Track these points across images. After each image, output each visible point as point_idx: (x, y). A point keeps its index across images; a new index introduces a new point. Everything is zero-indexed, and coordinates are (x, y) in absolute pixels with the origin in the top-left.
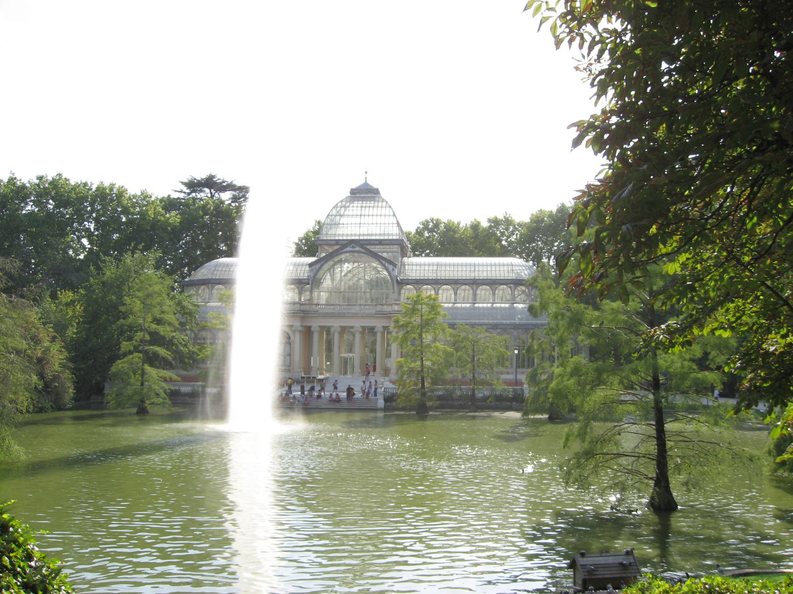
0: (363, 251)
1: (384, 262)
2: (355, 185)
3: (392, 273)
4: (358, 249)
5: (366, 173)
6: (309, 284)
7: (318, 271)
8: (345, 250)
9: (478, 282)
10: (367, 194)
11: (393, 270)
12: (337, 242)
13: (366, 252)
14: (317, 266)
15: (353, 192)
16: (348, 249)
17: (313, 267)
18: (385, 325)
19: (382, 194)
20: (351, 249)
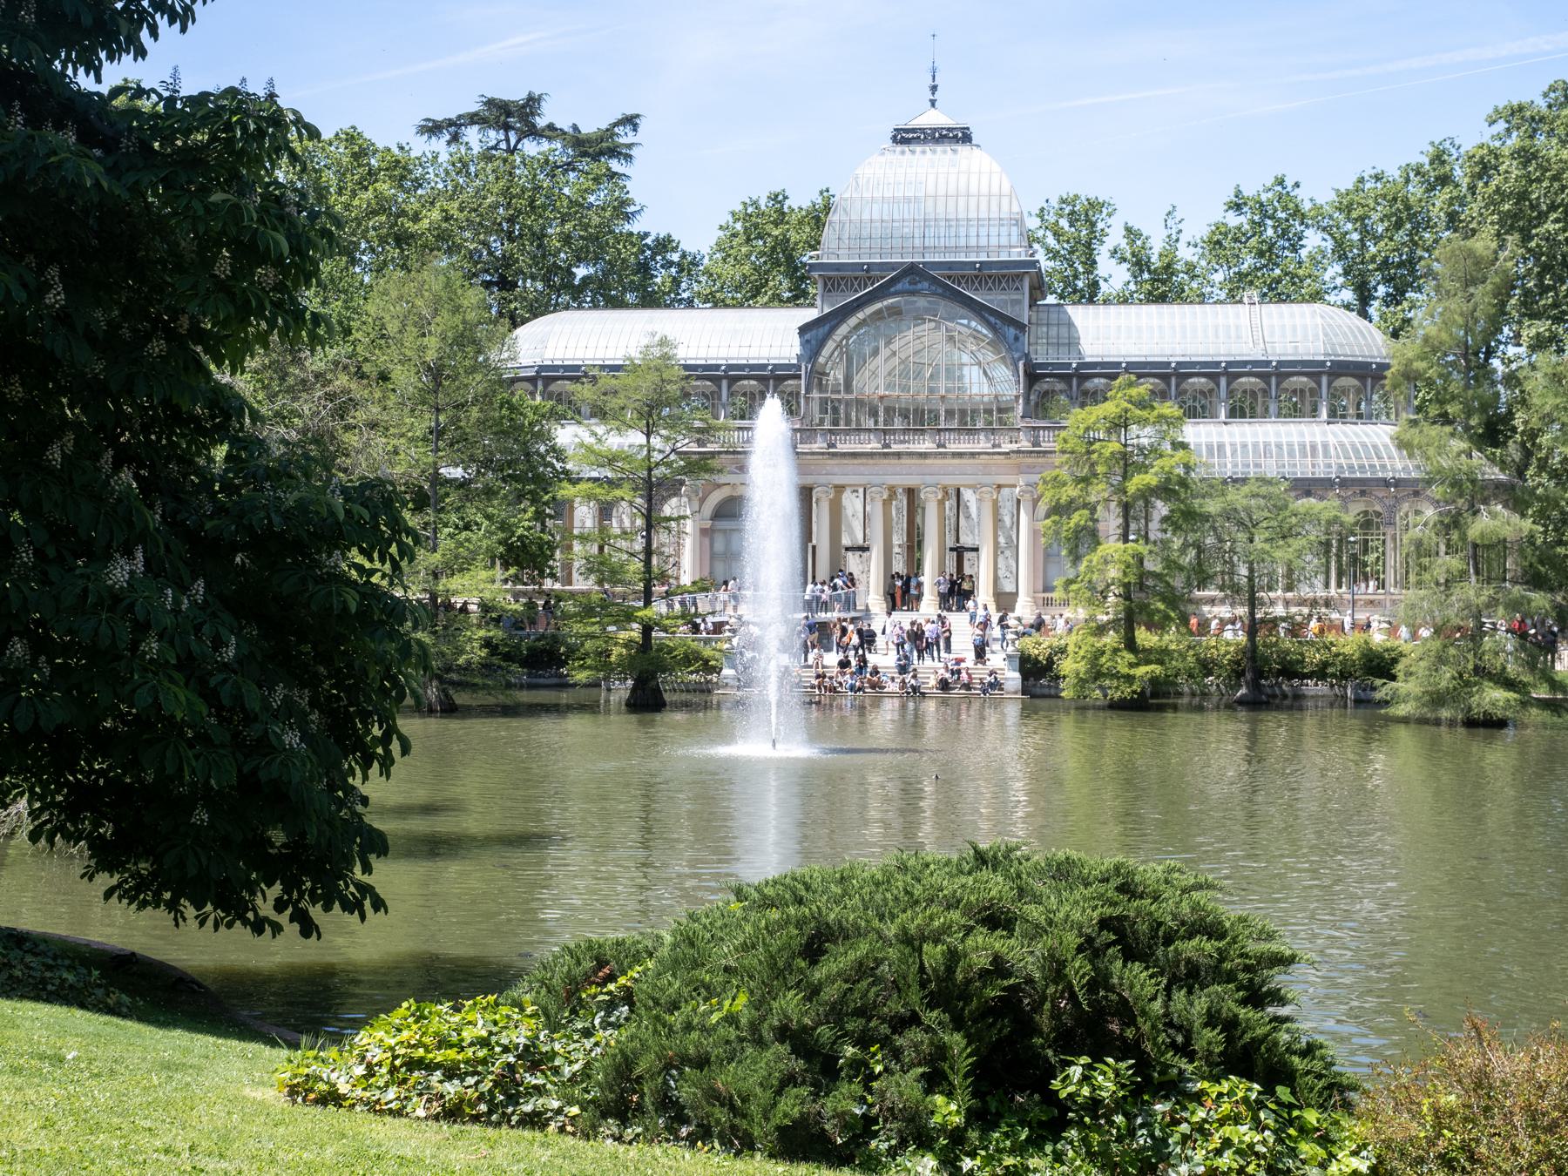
1: (992, 319)
6: (799, 377)
7: (822, 344)
8: (892, 290)
11: (1017, 339)
13: (948, 293)
14: (822, 331)
16: (899, 286)
17: (807, 336)
20: (907, 286)
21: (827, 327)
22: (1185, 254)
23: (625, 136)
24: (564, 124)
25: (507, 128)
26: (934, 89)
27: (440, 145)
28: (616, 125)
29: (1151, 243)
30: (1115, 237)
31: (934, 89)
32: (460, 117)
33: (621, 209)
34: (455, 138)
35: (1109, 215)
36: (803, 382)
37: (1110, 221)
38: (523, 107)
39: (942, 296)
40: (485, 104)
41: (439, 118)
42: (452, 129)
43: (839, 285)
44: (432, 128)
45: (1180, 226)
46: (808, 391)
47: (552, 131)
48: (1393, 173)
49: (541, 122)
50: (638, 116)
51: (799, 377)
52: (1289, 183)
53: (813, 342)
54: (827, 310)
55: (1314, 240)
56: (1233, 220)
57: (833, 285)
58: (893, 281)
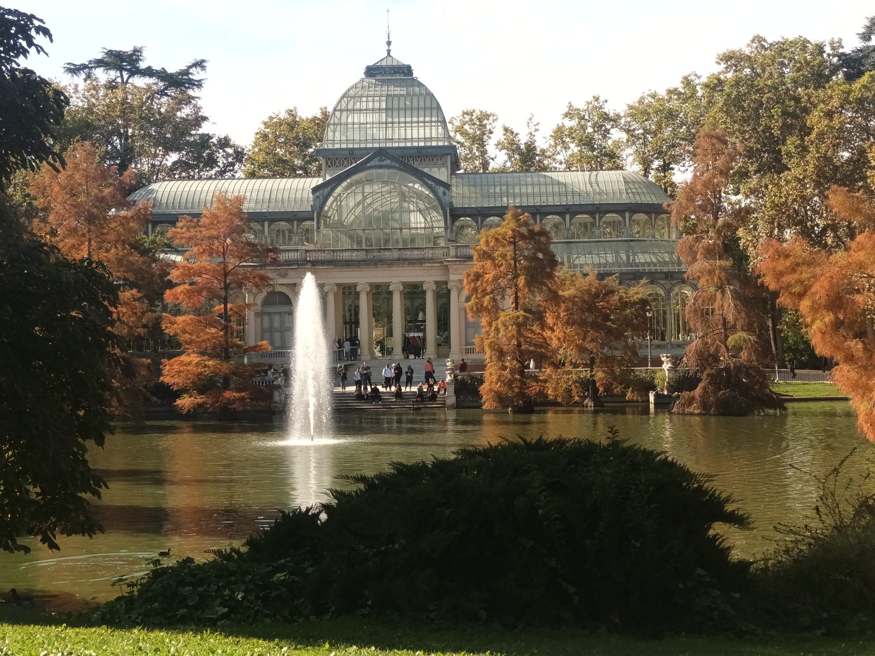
0: (397, 165)
1: (429, 182)
2: (371, 63)
3: (442, 199)
4: (388, 162)
6: (313, 219)
8: (368, 165)
9: (574, 209)
10: (392, 75)
12: (351, 154)
14: (326, 191)
15: (371, 71)
17: (317, 194)
18: (438, 279)
19: (415, 74)
20: (377, 163)
21: (329, 188)
22: (542, 143)
23: (196, 74)
24: (157, 67)
25: (121, 69)
26: (389, 43)
27: (79, 80)
28: (190, 67)
29: (520, 137)
30: (498, 135)
31: (389, 43)
32: (90, 62)
34: (89, 76)
35: (494, 121)
36: (315, 223)
37: (494, 125)
38: (131, 55)
40: (107, 54)
41: (78, 62)
42: (86, 70)
43: (335, 163)
44: (74, 70)
45: (537, 127)
46: (318, 228)
47: (149, 72)
48: (662, 93)
49: (143, 65)
50: (203, 61)
51: (313, 219)
52: (601, 100)
53: (321, 197)
54: (328, 178)
55: (617, 135)
56: (569, 123)
57: (331, 163)
58: (369, 160)
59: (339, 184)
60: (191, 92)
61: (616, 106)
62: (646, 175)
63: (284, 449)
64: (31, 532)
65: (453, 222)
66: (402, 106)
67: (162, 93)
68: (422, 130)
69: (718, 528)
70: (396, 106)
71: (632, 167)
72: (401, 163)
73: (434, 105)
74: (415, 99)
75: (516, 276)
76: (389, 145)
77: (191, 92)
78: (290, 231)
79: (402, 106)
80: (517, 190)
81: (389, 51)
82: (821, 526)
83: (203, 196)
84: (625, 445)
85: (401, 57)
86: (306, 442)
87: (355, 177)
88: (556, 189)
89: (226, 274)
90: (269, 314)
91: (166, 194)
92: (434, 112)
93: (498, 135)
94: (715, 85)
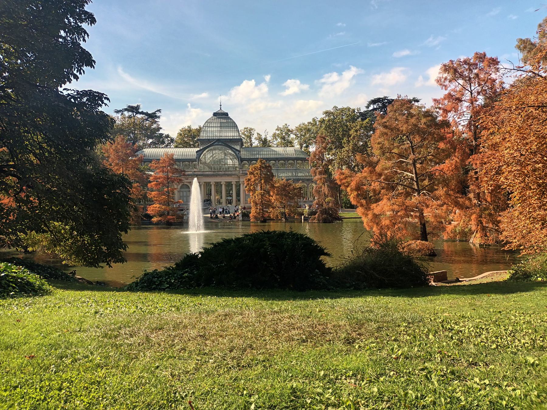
5: (221, 105)
9: (279, 159)
12: (209, 140)
14: (201, 152)
15: (215, 114)
22: (269, 138)
23: (158, 114)
24: (145, 111)
25: (133, 112)
27: (119, 115)
28: (156, 112)
33: (159, 129)
34: (122, 114)
39: (224, 146)
44: (117, 112)
46: (198, 164)
47: (142, 113)
48: (306, 123)
49: (140, 111)
52: (288, 125)
54: (201, 148)
55: (292, 136)
56: (277, 132)
59: (205, 150)
60: (156, 120)
61: (292, 127)
62: (301, 149)
63: (187, 234)
64: (103, 262)
65: (241, 163)
66: (225, 126)
67: (147, 120)
68: (231, 133)
69: (322, 257)
70: (223, 125)
71: (297, 146)
72: (225, 144)
73: (235, 125)
74: (229, 124)
75: (261, 180)
76: (221, 138)
77: (156, 120)
78: (189, 165)
79: (225, 126)
80: (261, 153)
81: (221, 108)
82: (353, 256)
83: (160, 153)
84: (294, 232)
85: (225, 110)
86: (194, 232)
87: (210, 148)
88: (273, 153)
89: (168, 179)
90: (182, 191)
91: (148, 153)
92: (235, 128)
93: (255, 135)
94: (322, 121)
